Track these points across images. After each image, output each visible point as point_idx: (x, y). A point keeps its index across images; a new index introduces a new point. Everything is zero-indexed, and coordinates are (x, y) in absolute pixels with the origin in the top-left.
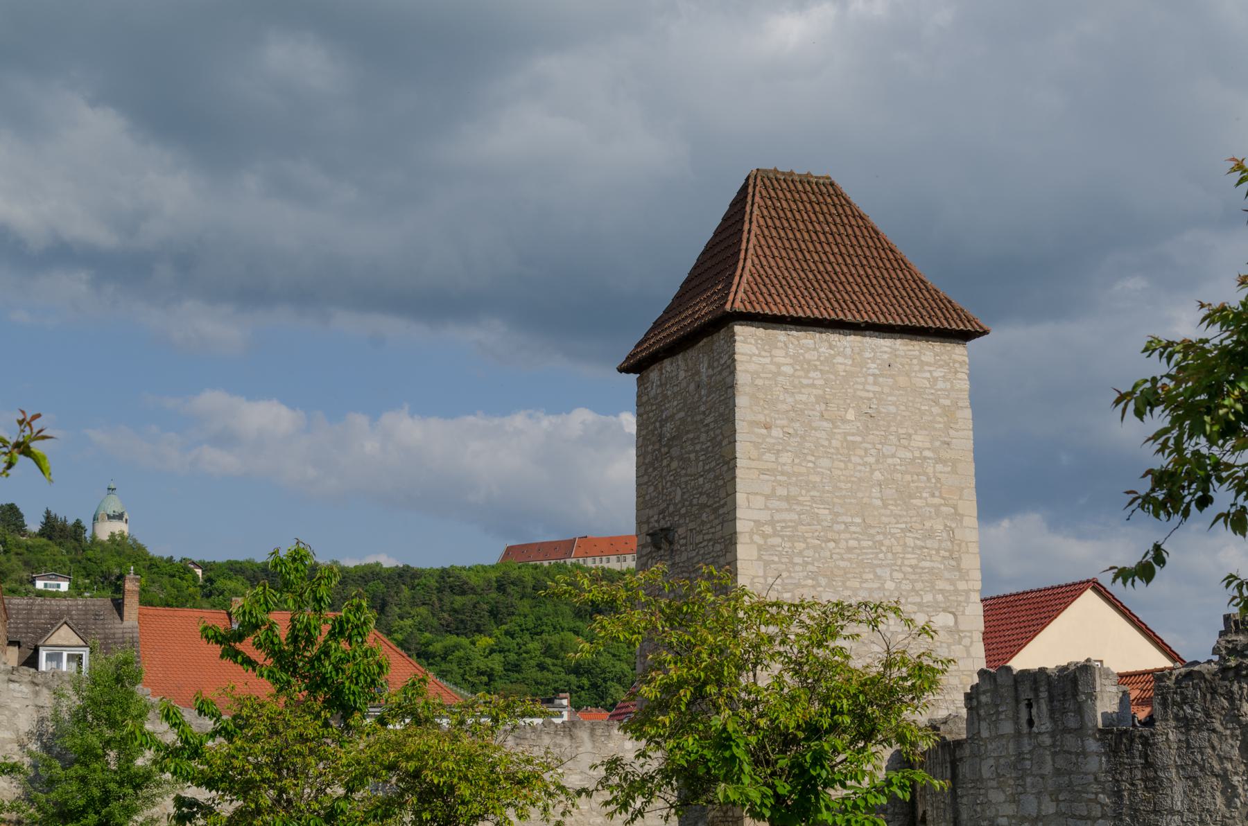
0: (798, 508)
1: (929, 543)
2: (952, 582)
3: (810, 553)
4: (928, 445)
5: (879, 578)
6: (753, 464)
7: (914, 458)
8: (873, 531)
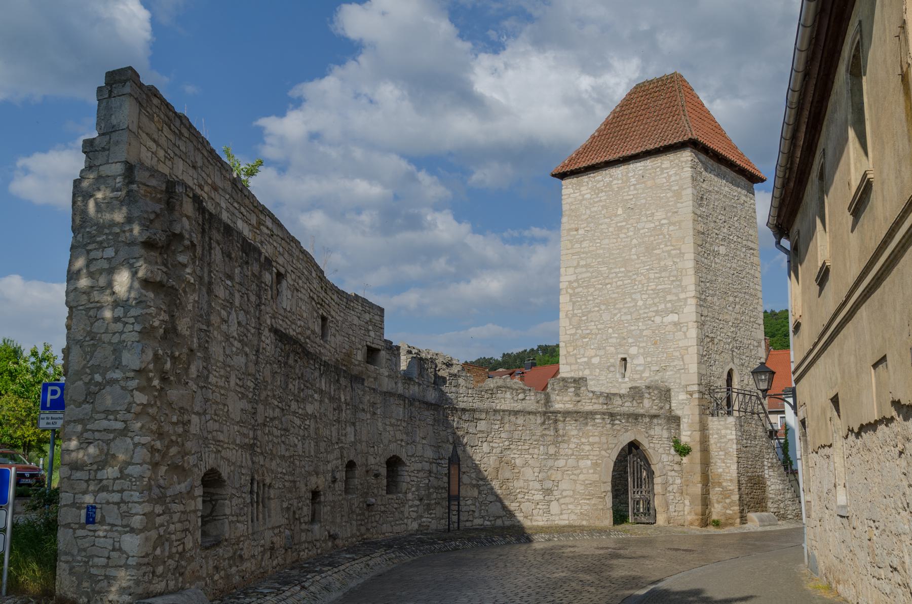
0: (591, 270)
1: (663, 274)
2: (677, 295)
3: (597, 293)
4: (664, 216)
5: (633, 300)
6: (569, 251)
7: (656, 226)
8: (631, 274)
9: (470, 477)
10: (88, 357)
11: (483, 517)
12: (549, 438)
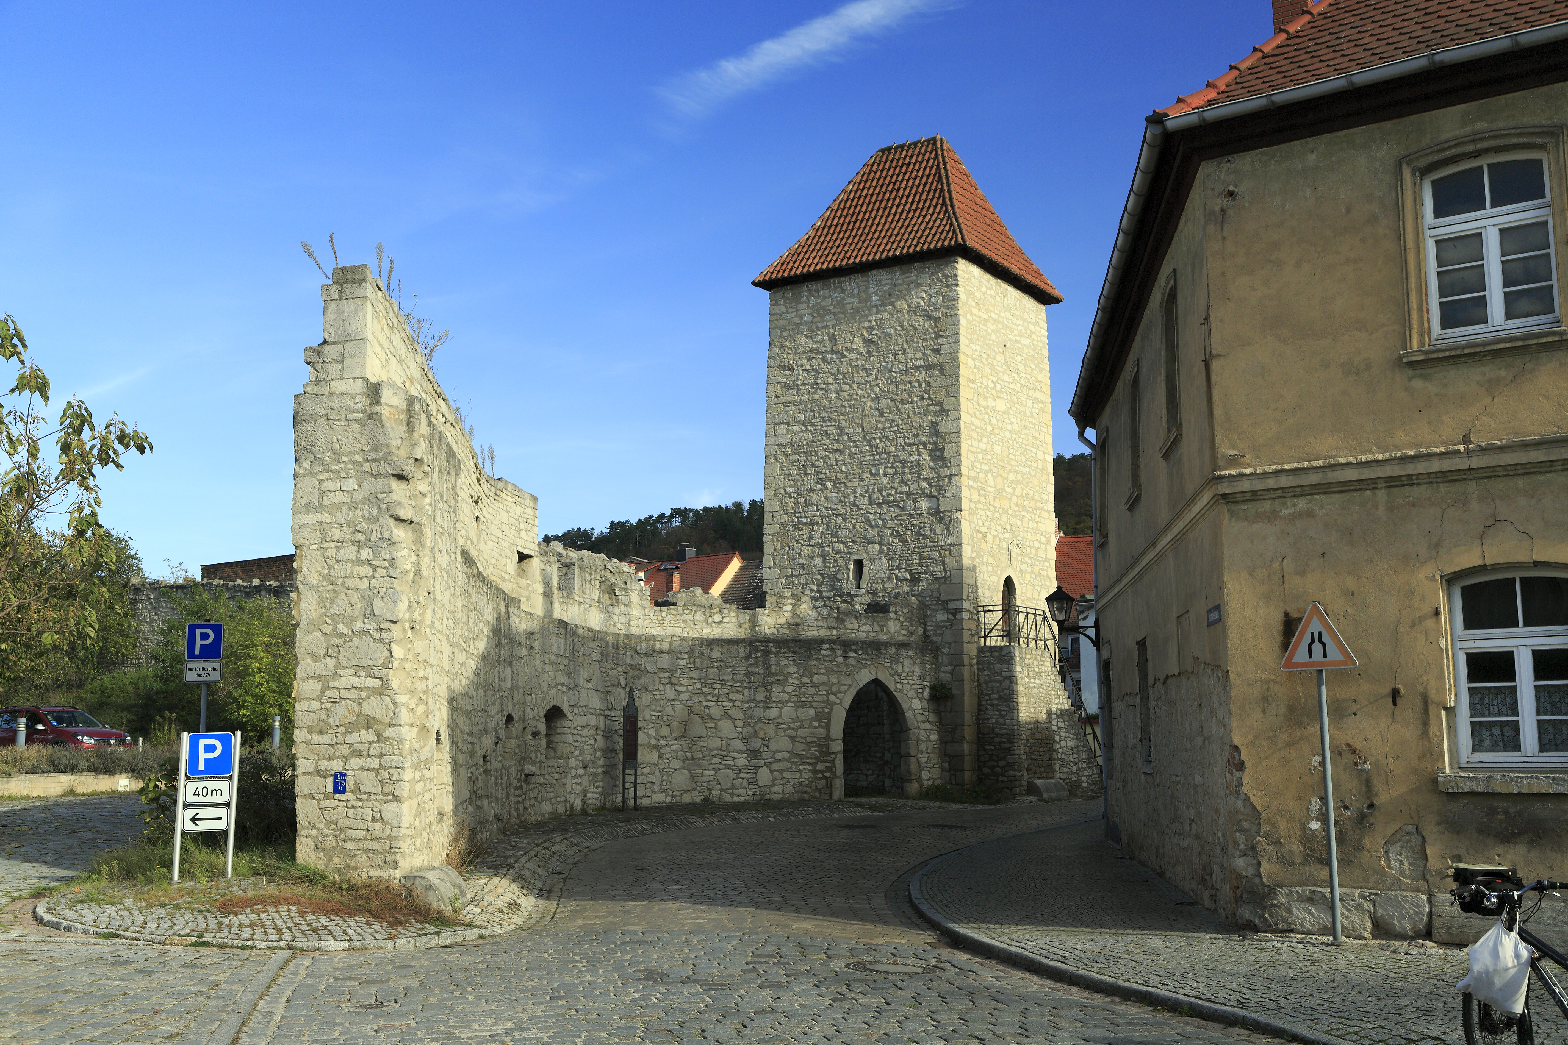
9: (647, 734)
10: (328, 605)
11: (664, 791)
12: (757, 678)
